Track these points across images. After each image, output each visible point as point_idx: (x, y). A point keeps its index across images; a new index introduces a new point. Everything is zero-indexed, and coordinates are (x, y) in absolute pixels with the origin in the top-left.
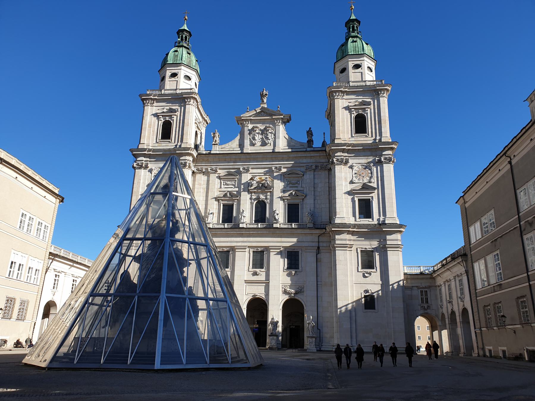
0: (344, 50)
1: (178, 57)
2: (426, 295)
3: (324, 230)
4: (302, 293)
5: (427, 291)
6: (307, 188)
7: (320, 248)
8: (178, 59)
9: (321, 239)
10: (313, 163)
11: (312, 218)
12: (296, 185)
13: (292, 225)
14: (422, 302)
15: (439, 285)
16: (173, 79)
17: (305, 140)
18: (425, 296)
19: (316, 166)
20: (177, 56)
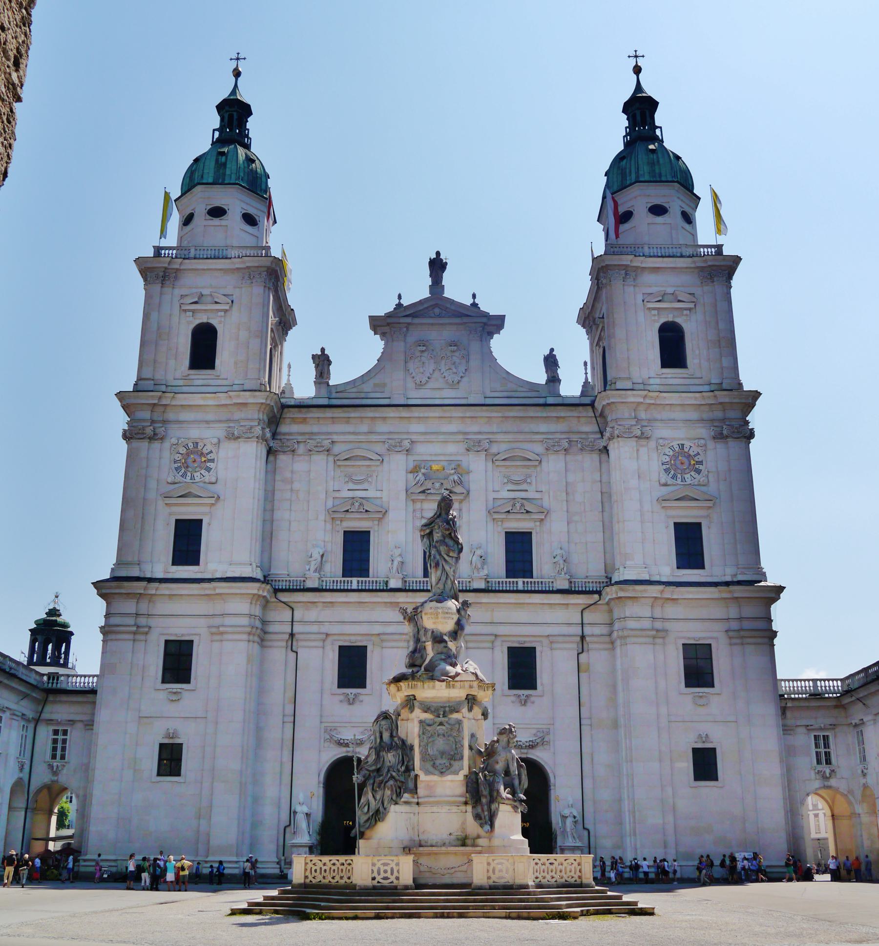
0: (625, 168)
1: (227, 170)
2: (827, 745)
3: (596, 596)
4: (545, 747)
5: (827, 736)
6: (551, 494)
7: (587, 639)
8: (228, 172)
9: (588, 617)
10: (562, 433)
11: (567, 567)
12: (524, 487)
14: (819, 762)
15: (857, 721)
16: (216, 221)
17: (540, 377)
18: (825, 747)
19: (570, 442)
20: (224, 165)
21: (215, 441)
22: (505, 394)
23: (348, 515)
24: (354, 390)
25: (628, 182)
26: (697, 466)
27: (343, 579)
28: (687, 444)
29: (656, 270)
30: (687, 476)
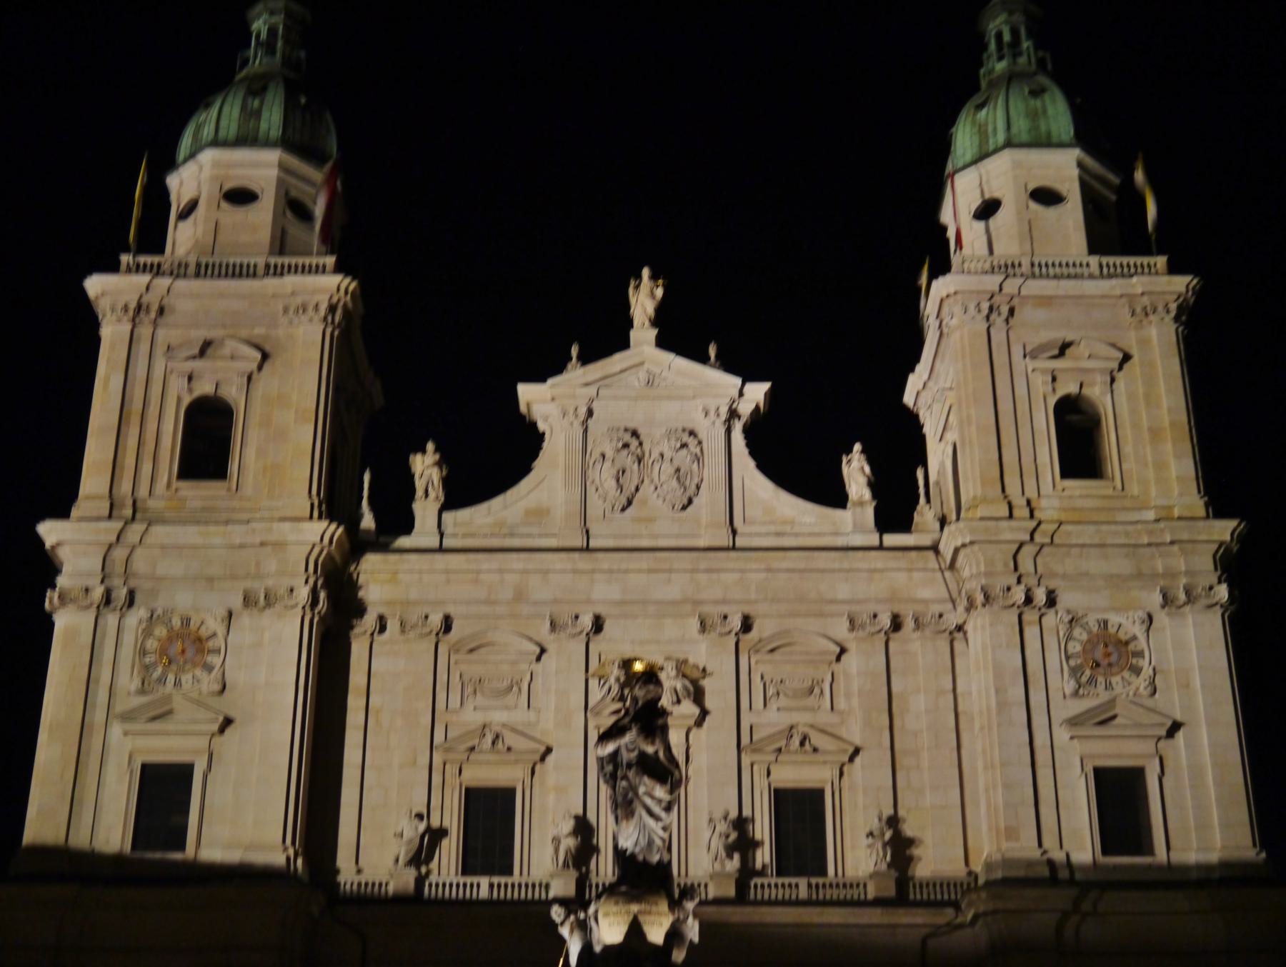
0: (986, 124)
1: (262, 122)
3: (950, 912)
8: (264, 126)
12: (811, 701)
13: (797, 886)
20: (257, 114)
21: (222, 612)
22: (772, 528)
23: (473, 757)
24: (489, 520)
25: (991, 147)
26: (1134, 661)
27: (462, 880)
28: (1114, 619)
29: (1045, 301)
30: (1116, 680)
